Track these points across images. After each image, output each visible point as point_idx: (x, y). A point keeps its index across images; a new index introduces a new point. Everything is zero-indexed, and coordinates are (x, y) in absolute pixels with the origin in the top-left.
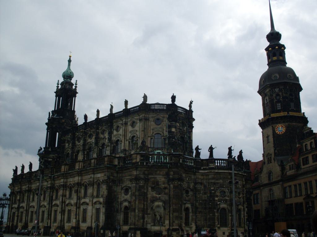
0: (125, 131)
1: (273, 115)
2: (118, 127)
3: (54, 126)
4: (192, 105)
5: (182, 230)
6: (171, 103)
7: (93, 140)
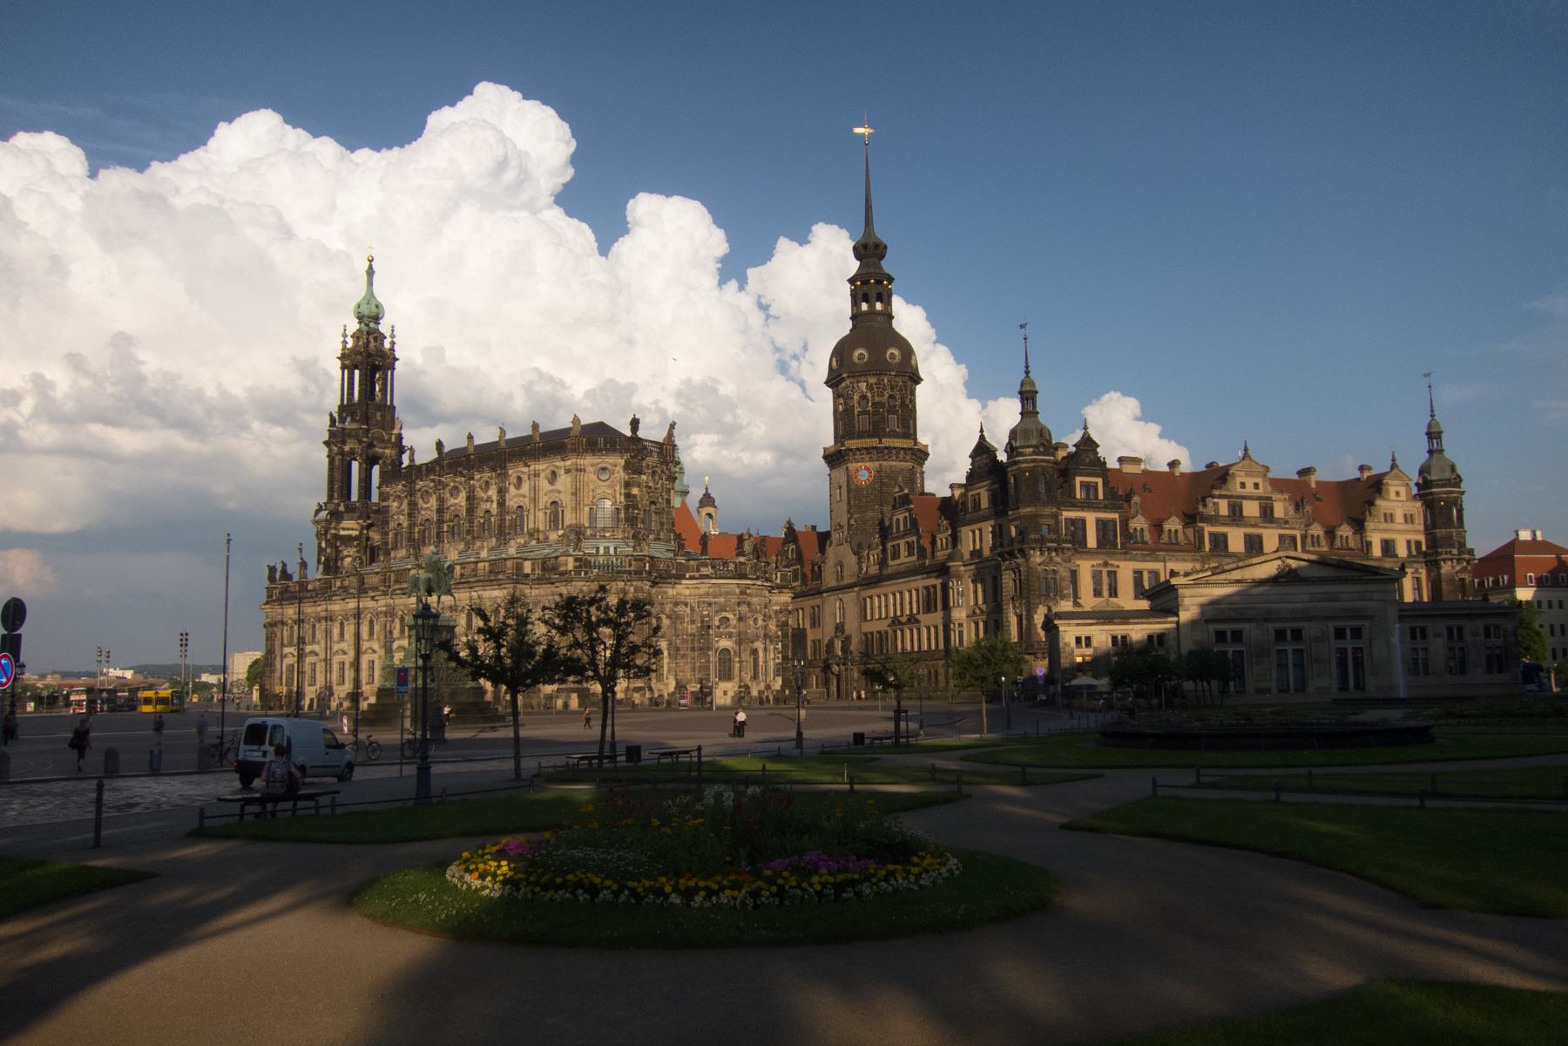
0: (535, 489)
1: (853, 444)
2: (519, 479)
3: (347, 448)
4: (676, 432)
5: (651, 690)
6: (628, 433)
7: (461, 500)
